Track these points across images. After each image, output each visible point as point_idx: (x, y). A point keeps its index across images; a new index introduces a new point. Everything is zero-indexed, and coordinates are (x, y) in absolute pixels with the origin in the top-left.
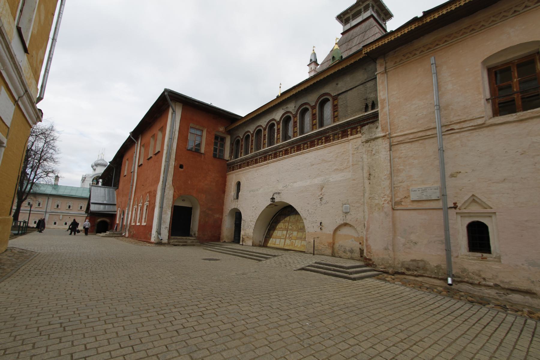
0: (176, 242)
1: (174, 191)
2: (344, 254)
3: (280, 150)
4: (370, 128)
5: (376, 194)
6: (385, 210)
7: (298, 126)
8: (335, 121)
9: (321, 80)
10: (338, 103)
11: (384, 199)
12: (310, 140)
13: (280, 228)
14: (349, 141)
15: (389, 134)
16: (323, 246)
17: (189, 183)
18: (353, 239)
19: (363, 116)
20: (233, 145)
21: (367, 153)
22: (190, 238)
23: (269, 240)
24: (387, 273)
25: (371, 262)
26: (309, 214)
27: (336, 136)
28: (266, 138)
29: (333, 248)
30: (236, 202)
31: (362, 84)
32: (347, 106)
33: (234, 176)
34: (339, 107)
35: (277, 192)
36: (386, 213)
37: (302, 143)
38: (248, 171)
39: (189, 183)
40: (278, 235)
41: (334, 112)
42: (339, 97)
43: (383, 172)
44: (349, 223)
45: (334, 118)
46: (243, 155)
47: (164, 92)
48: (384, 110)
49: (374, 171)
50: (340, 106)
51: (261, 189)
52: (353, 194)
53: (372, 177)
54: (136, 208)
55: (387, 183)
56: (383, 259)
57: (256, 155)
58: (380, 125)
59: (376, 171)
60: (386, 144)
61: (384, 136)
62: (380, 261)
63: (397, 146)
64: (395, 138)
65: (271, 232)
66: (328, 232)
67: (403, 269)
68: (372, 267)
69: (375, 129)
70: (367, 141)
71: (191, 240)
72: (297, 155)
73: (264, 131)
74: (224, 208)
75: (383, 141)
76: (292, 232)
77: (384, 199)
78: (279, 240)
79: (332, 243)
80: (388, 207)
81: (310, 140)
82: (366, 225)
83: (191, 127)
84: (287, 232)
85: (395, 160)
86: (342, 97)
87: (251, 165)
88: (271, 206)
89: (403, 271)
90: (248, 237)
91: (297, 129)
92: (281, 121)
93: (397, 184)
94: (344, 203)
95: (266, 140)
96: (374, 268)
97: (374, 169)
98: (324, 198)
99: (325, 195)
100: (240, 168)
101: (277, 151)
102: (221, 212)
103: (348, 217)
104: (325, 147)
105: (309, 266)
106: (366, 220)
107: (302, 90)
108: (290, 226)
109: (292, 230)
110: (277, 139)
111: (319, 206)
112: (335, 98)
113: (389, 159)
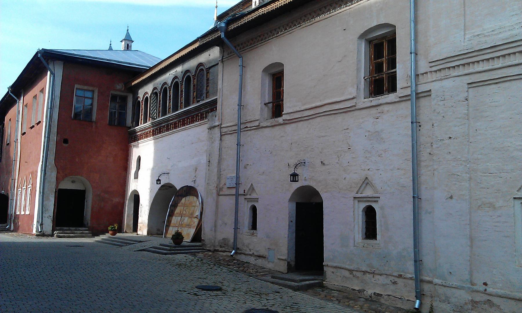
47: (37, 53)
54: (21, 191)
101: (169, 123)
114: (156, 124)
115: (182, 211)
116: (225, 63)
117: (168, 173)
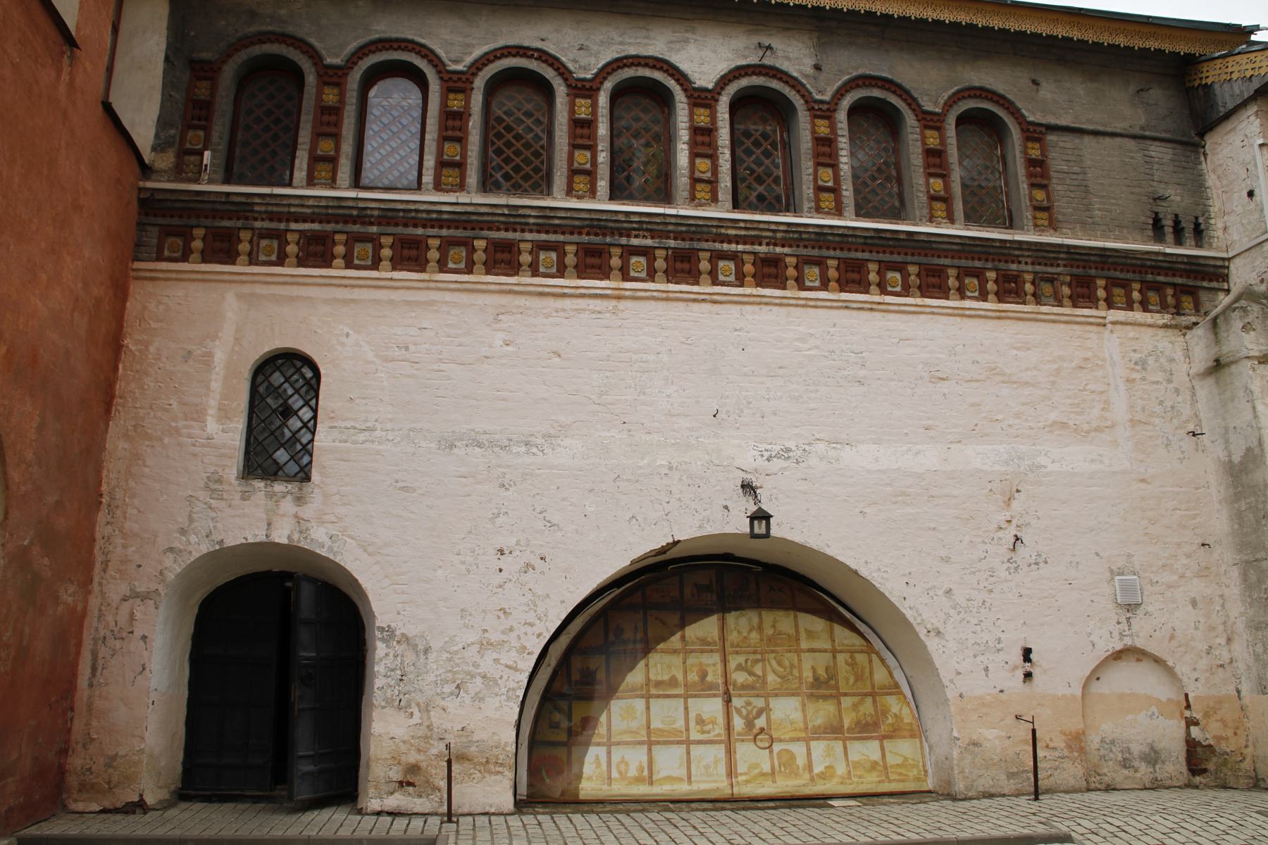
2: (1126, 772)
3: (726, 246)
12: (923, 260)
13: (659, 684)
18: (1154, 709)
31: (1134, 137)
32: (1086, 190)
37: (875, 256)
38: (408, 303)
44: (1148, 649)
52: (1146, 534)
66: (1062, 690)
74: (101, 530)
76: (760, 703)
84: (728, 701)
86: (1061, 144)
99: (1028, 524)
108: (739, 668)
109: (757, 688)
111: (1003, 573)
112: (1035, 133)
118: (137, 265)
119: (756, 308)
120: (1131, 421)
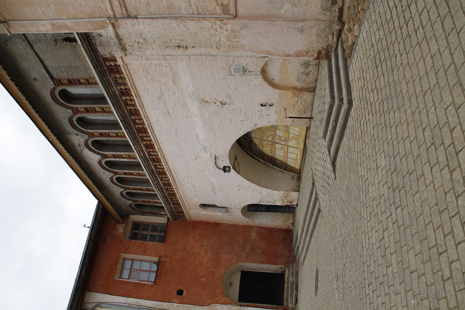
0: (292, 298)
1: (217, 303)
2: (311, 75)
4: (101, 45)
5: (211, 40)
6: (237, 28)
7: (107, 131)
8: (94, 82)
9: (31, 104)
10: (65, 79)
11: (218, 29)
13: (271, 152)
14: (126, 65)
15: (109, 18)
16: (299, 104)
17: (204, 280)
19: (84, 46)
20: (145, 212)
21: (143, 49)
22: (286, 276)
23: (291, 166)
24: (340, 32)
25: (324, 52)
26: (247, 120)
27: (120, 81)
28: (130, 171)
29: (301, 90)
30: (231, 210)
31: (32, 46)
33: (191, 211)
34: (71, 77)
35: (213, 164)
36: (242, 28)
38: (184, 194)
39: (204, 280)
40: (282, 155)
41: (80, 84)
42: (55, 77)
43: (174, 29)
45: (89, 83)
46: (158, 201)
48: (70, 25)
49: (173, 41)
50: (70, 75)
51: (211, 178)
53: (182, 44)
55: (192, 25)
56: (318, 35)
57: (157, 185)
58: (95, 31)
59: (171, 38)
60: (126, 23)
61: (113, 26)
62: (321, 40)
63: (128, 8)
64: (115, 11)
65: (277, 162)
67: (334, 9)
68: (331, 51)
69: (103, 38)
70: (124, 49)
71: (289, 275)
72: (153, 132)
73: (119, 174)
74: (241, 224)
75: (121, 27)
76: (277, 137)
77: (218, 29)
78: (289, 154)
79: (293, 91)
80: (231, 25)
81: (128, 116)
82: (264, 55)
83: (120, 278)
84: (277, 143)
85: (152, 11)
86: (56, 73)
87: (174, 191)
88: (236, 166)
89: (337, 10)
90: (286, 197)
91: (113, 133)
92: (102, 152)
93: (193, 10)
94: (229, 74)
95: (133, 172)
96: (333, 49)
97: (169, 40)
98: (221, 99)
99: (215, 98)
100: (179, 204)
101: (148, 158)
102: (249, 228)
103: (251, 67)
104: (138, 96)
105: (329, 151)
106: (255, 54)
107: (49, 128)
108: (267, 138)
109: (274, 136)
110: (130, 158)
111: (234, 107)
113: (151, 20)
114: (155, 179)
115: (268, 143)
116: (7, 17)
117: (216, 157)
118: (188, 219)
119: (162, 149)
120: (165, 60)
